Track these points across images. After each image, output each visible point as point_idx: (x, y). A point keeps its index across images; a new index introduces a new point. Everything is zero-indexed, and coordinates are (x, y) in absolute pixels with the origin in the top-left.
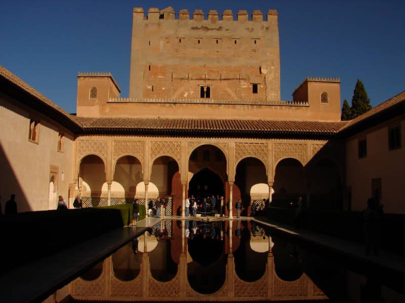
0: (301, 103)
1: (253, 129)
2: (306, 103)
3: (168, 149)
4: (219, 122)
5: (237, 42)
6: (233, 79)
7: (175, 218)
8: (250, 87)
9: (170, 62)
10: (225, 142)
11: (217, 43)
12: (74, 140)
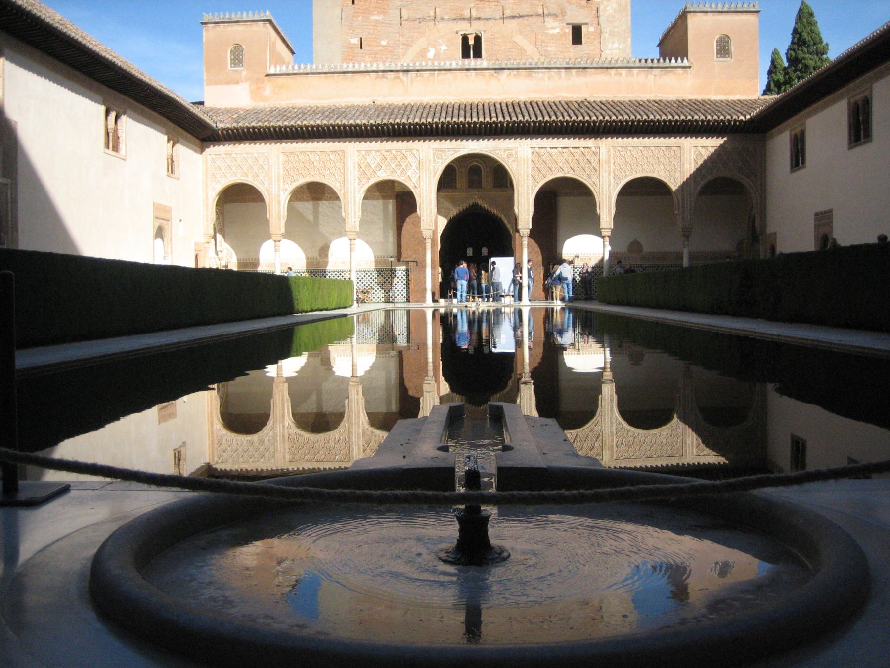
0: (673, 61)
1: (567, 118)
2: (682, 61)
3: (393, 165)
4: (498, 106)
6: (531, 16)
7: (413, 306)
8: (567, 30)
10: (510, 147)
12: (202, 151)
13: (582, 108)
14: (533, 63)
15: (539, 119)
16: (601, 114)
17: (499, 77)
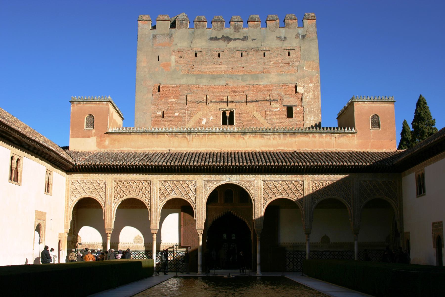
0: (346, 129)
1: (284, 164)
4: (244, 155)
5: (266, 55)
8: (284, 110)
9: (183, 81)
11: (242, 56)
13: (293, 157)
14: (264, 130)
16: (305, 161)
17: (244, 138)
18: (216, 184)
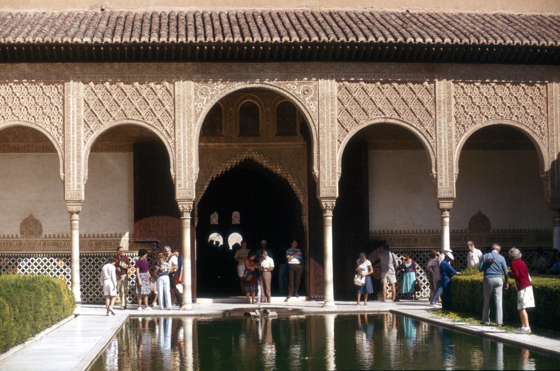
15: (350, 40)
18: (222, 88)
